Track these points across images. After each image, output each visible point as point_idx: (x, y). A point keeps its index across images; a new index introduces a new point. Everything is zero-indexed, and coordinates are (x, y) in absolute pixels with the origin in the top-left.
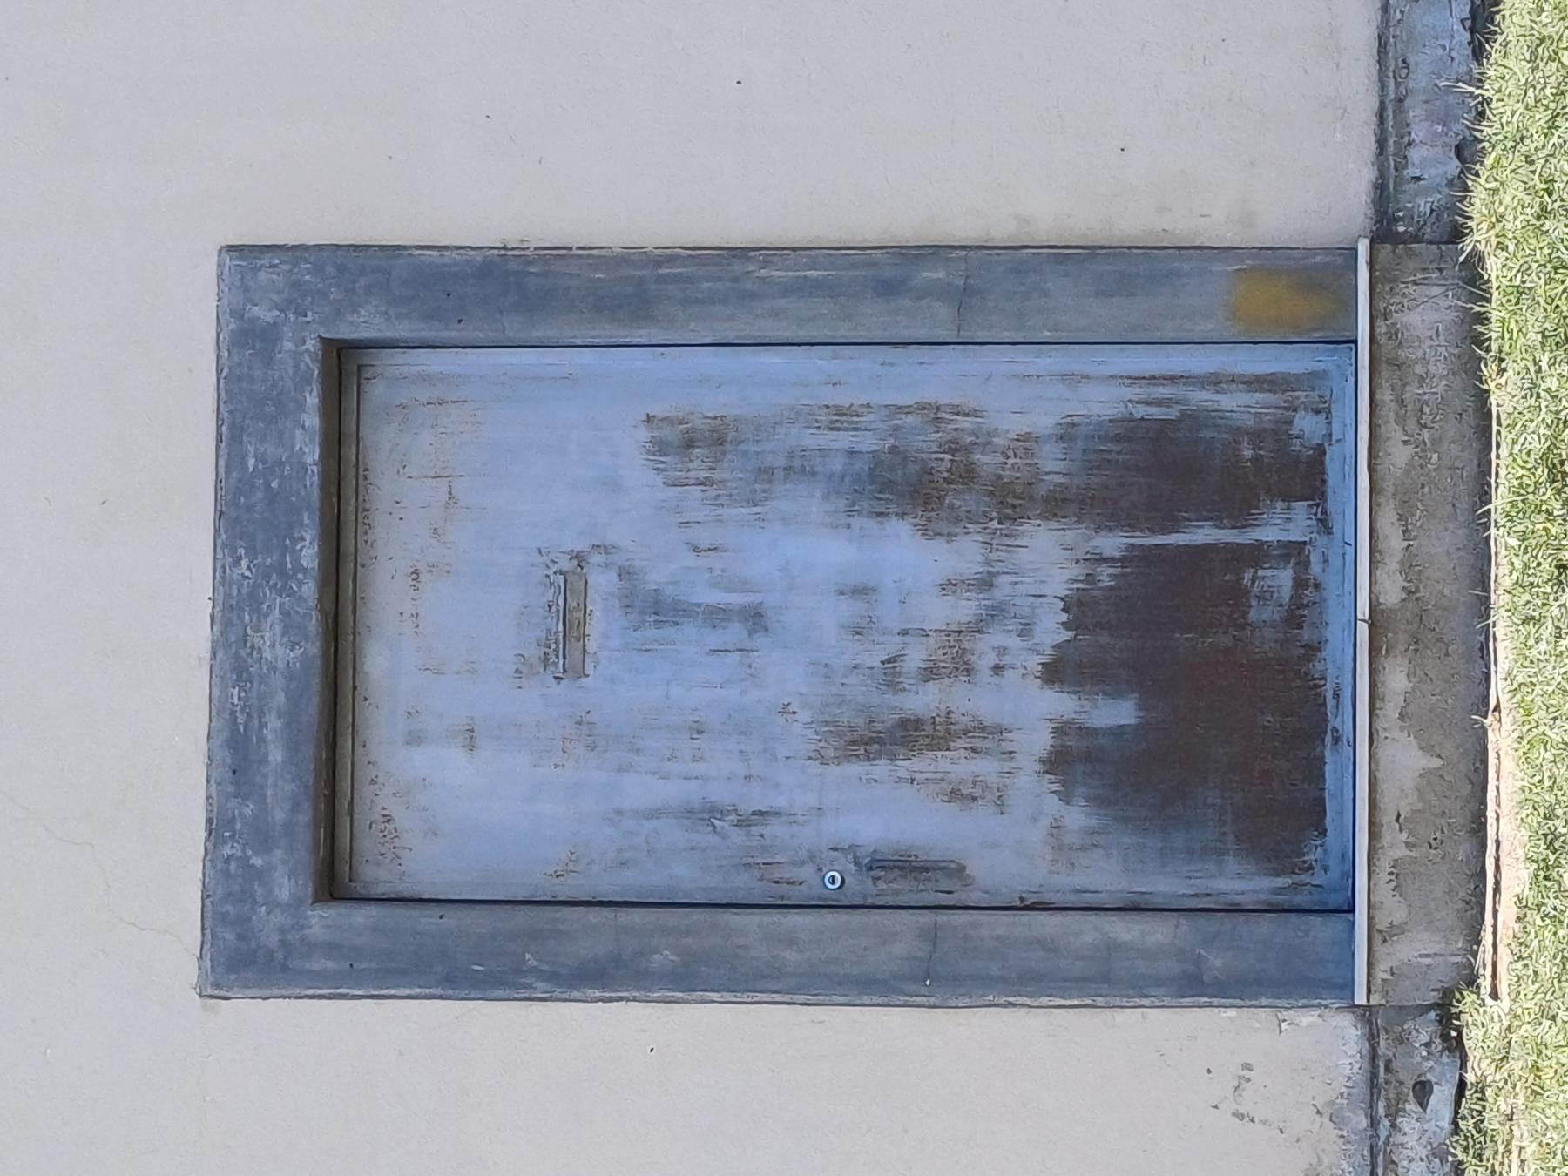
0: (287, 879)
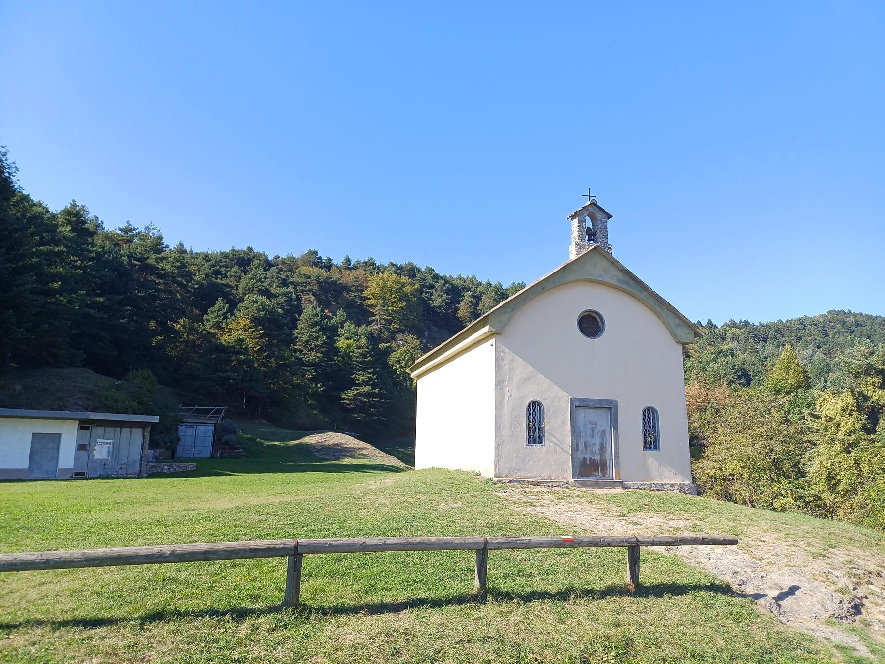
0: (577, 403)
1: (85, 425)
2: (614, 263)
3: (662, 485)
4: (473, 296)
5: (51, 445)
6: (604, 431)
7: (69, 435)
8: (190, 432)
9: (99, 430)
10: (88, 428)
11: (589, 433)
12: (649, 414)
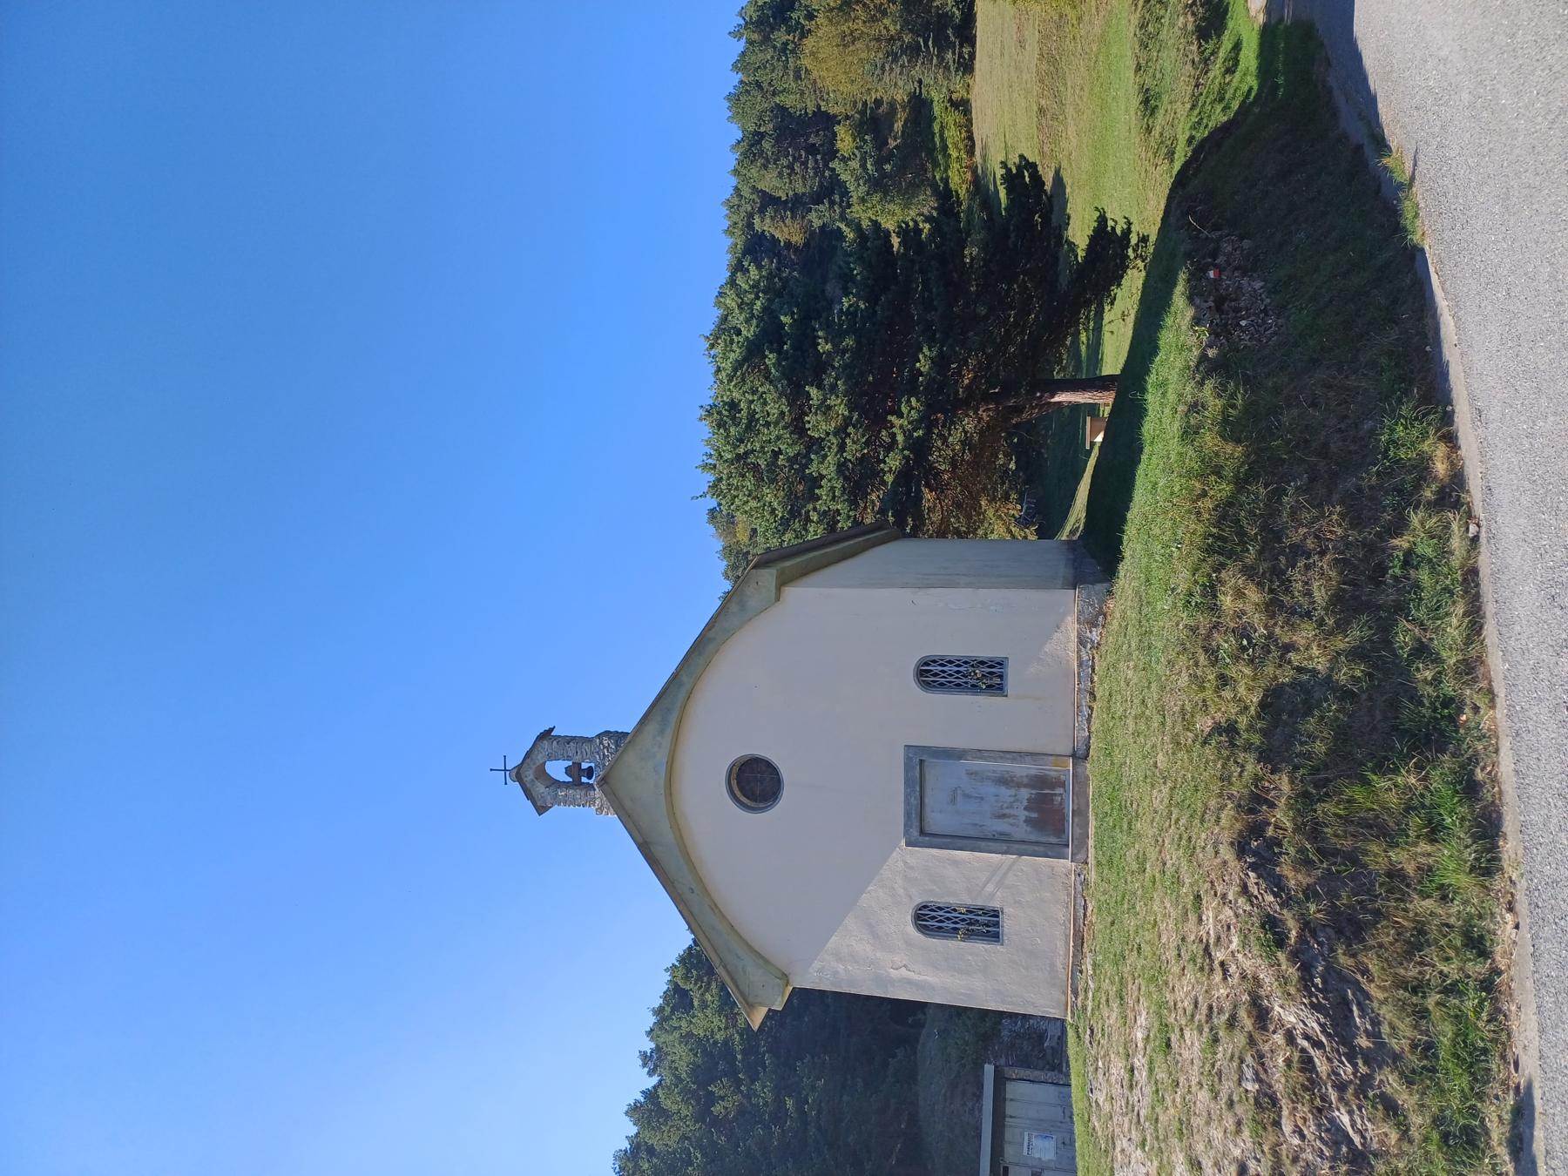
0: (915, 833)
3: (1080, 665)
4: (762, 211)
6: (970, 773)
9: (1010, 1152)
12: (935, 674)
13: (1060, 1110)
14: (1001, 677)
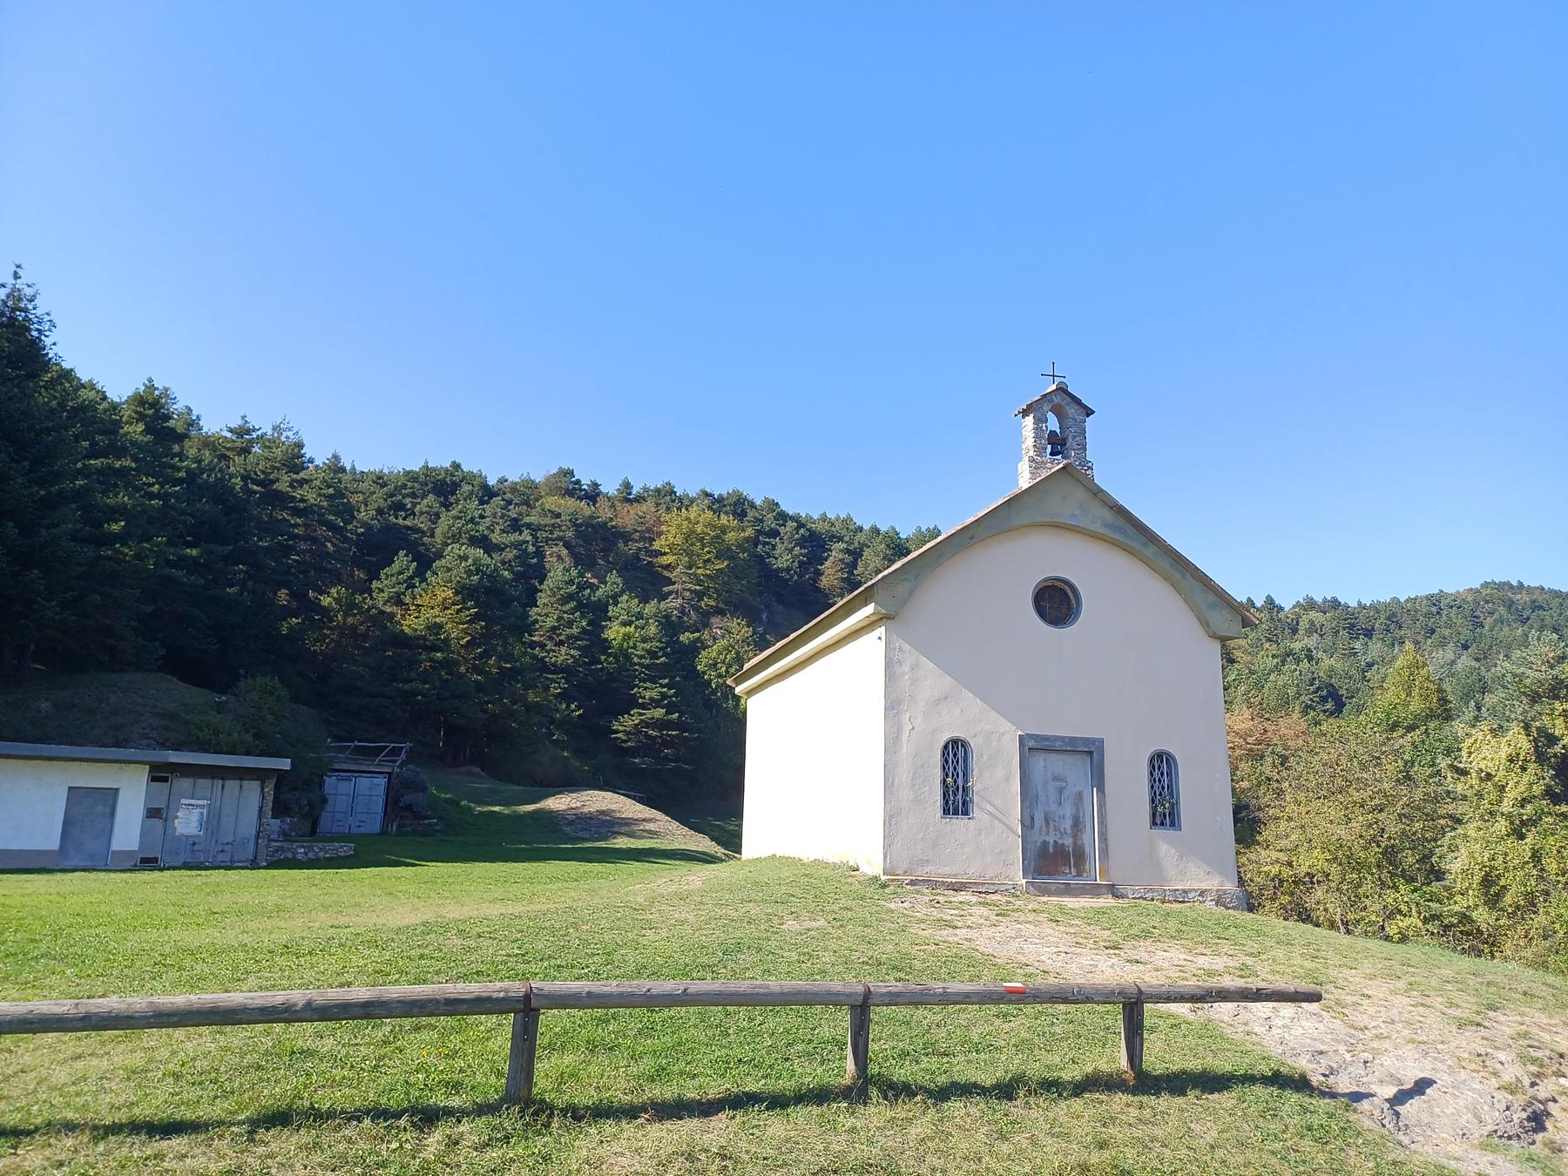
0: (1032, 744)
1: (160, 774)
2: (1097, 493)
3: (1185, 892)
4: (848, 551)
5: (99, 808)
6: (1080, 794)
7: (132, 790)
8: (345, 787)
9: (185, 783)
10: (165, 780)
11: (1053, 797)
12: (1162, 765)
13: (229, 839)
14: (1162, 824)
